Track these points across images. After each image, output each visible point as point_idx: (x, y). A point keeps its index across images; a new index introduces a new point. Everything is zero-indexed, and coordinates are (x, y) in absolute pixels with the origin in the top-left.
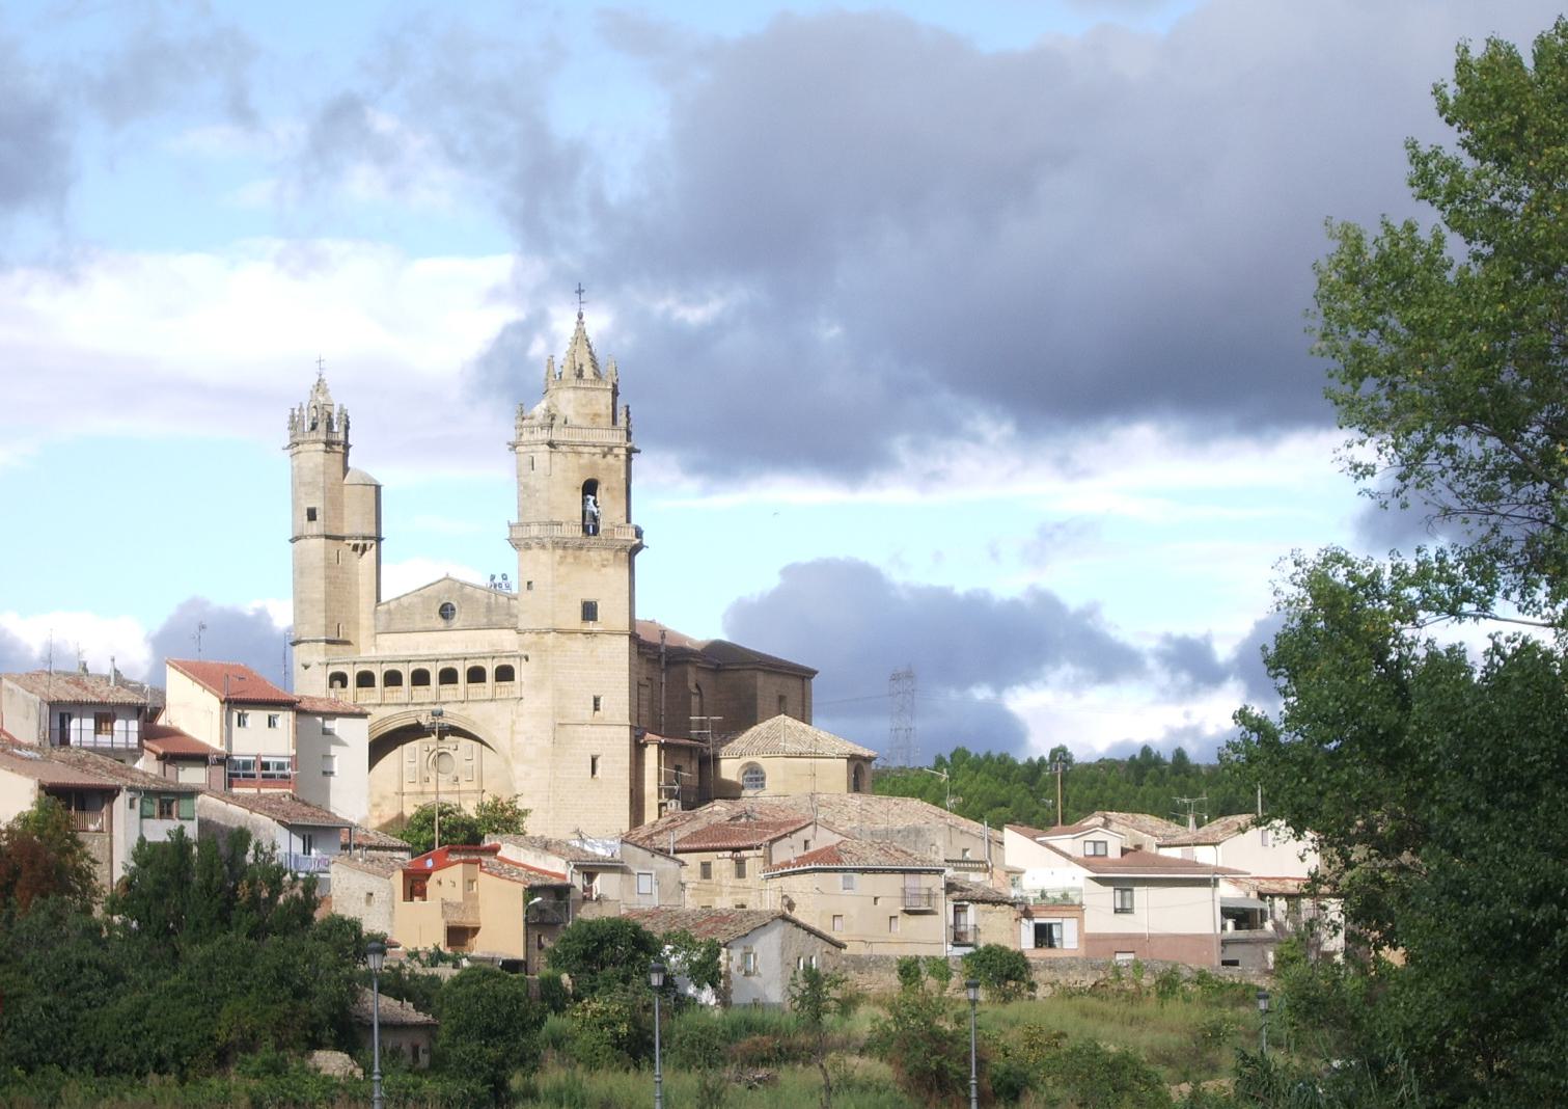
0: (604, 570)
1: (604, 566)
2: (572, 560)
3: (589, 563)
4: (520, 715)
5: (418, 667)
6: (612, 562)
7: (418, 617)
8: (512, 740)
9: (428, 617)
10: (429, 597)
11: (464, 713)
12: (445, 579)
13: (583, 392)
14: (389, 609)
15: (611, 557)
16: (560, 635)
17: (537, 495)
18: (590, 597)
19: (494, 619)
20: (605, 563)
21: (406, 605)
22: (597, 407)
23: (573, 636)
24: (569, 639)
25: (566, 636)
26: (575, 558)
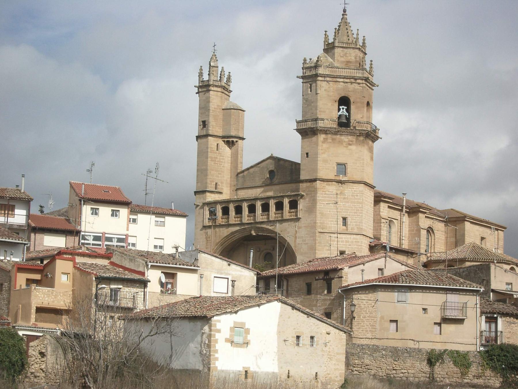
0: (350, 147)
1: (350, 145)
2: (331, 141)
3: (341, 142)
4: (299, 228)
6: (354, 142)
8: (295, 241)
13: (341, 49)
15: (354, 140)
16: (322, 182)
17: (312, 105)
18: (341, 160)
20: (351, 143)
22: (349, 58)
23: (330, 183)
24: (327, 185)
25: (325, 183)
26: (333, 139)
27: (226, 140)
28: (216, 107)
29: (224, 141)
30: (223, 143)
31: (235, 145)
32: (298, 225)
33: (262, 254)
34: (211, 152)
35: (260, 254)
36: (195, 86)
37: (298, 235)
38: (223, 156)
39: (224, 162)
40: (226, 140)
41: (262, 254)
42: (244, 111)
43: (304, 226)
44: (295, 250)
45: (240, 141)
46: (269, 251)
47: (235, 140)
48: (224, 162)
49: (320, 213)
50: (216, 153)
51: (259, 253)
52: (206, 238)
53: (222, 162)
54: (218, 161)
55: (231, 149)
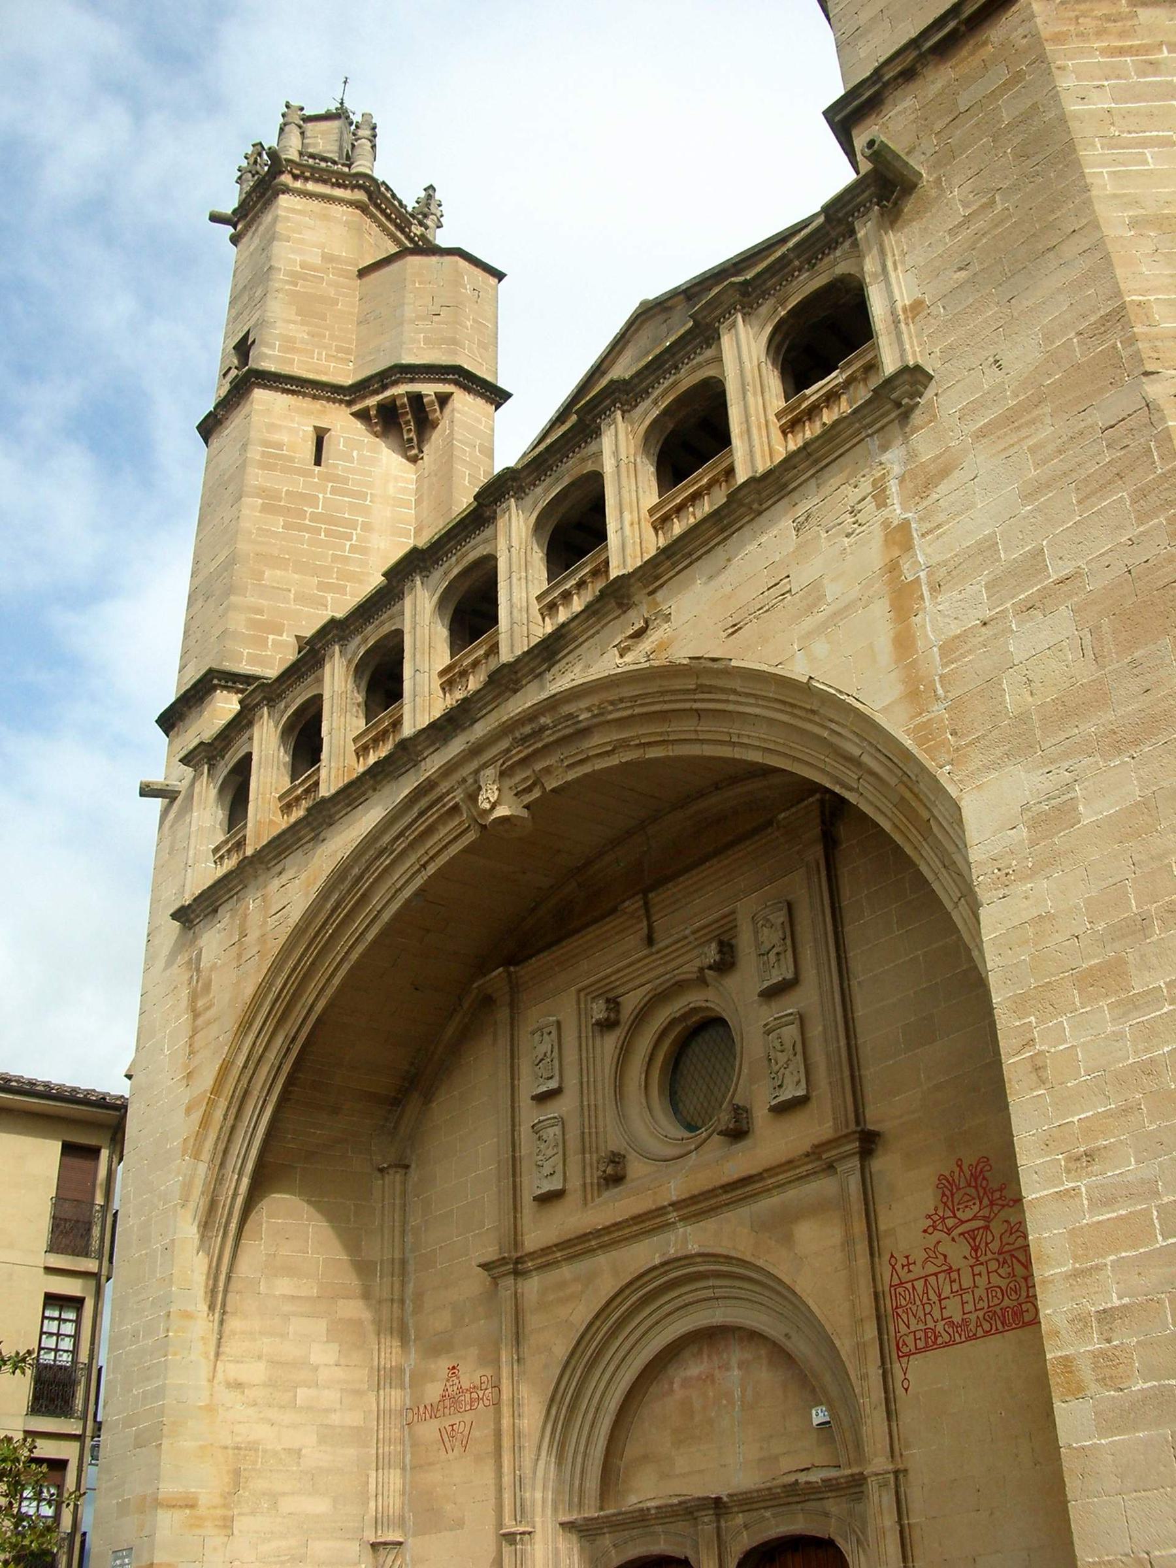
27: (372, 401)
28: (318, 261)
29: (362, 415)
30: (359, 425)
31: (434, 425)
32: (912, 456)
33: (644, 1044)
34: (265, 466)
35: (624, 1052)
36: (215, 218)
37: (925, 552)
38: (363, 496)
39: (367, 527)
40: (372, 401)
41: (644, 1044)
42: (500, 276)
43: (981, 434)
44: (924, 733)
45: (464, 403)
46: (694, 999)
47: (429, 389)
48: (367, 527)
49: (1134, 223)
50: (310, 474)
51: (610, 1043)
52: (194, 997)
53: (353, 525)
54: (314, 517)
55: (414, 460)
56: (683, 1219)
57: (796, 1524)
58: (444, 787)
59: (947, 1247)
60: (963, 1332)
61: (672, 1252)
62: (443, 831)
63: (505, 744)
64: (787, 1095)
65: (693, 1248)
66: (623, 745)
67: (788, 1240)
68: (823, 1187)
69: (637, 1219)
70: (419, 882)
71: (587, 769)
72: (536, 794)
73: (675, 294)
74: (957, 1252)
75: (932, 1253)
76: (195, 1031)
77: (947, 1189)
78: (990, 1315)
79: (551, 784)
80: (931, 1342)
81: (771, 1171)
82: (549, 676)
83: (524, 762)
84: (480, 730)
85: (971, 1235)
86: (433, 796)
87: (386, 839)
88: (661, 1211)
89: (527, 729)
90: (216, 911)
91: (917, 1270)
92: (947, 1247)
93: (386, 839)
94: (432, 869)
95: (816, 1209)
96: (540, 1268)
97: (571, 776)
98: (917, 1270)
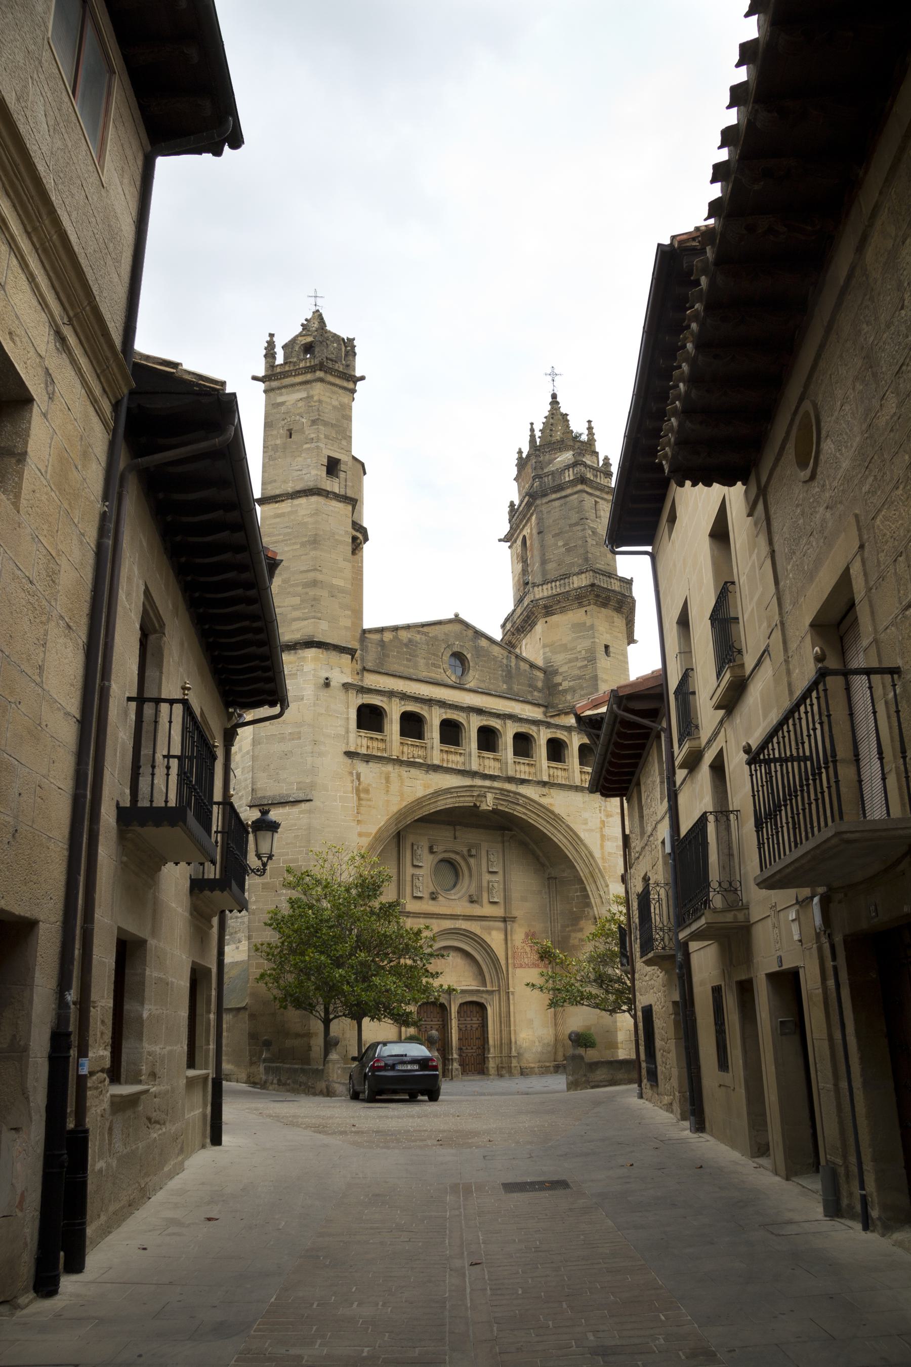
5: (485, 723)
7: (422, 662)
9: (434, 665)
10: (435, 638)
11: (544, 801)
12: (450, 621)
14: (382, 641)
19: (516, 687)
21: (405, 641)
56: (463, 919)
57: (474, 999)
58: (476, 789)
59: (525, 947)
60: (528, 966)
61: (457, 926)
62: (467, 799)
63: (497, 792)
64: (495, 900)
65: (463, 927)
66: (524, 814)
67: (490, 934)
68: (501, 925)
69: (451, 915)
70: (451, 806)
71: (511, 811)
72: (495, 807)
73: (473, 628)
74: (528, 949)
75: (523, 948)
76: (359, 806)
77: (527, 935)
78: (533, 964)
79: (500, 808)
80: (521, 966)
81: (491, 917)
82: (520, 786)
83: (498, 799)
84: (496, 784)
85: (531, 946)
86: (472, 789)
87: (453, 790)
88: (460, 915)
89: (506, 793)
90: (367, 762)
91: (519, 950)
92: (525, 947)
93: (453, 790)
94: (457, 805)
95: (498, 929)
96: (413, 917)
97: (506, 810)
98: (519, 950)
